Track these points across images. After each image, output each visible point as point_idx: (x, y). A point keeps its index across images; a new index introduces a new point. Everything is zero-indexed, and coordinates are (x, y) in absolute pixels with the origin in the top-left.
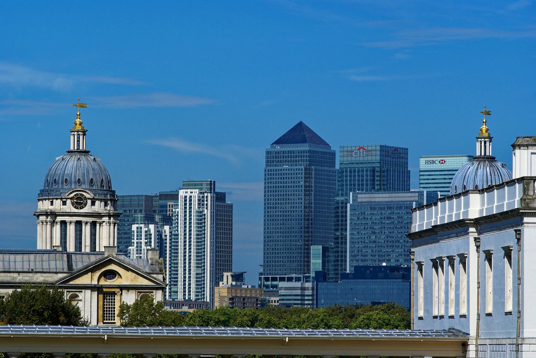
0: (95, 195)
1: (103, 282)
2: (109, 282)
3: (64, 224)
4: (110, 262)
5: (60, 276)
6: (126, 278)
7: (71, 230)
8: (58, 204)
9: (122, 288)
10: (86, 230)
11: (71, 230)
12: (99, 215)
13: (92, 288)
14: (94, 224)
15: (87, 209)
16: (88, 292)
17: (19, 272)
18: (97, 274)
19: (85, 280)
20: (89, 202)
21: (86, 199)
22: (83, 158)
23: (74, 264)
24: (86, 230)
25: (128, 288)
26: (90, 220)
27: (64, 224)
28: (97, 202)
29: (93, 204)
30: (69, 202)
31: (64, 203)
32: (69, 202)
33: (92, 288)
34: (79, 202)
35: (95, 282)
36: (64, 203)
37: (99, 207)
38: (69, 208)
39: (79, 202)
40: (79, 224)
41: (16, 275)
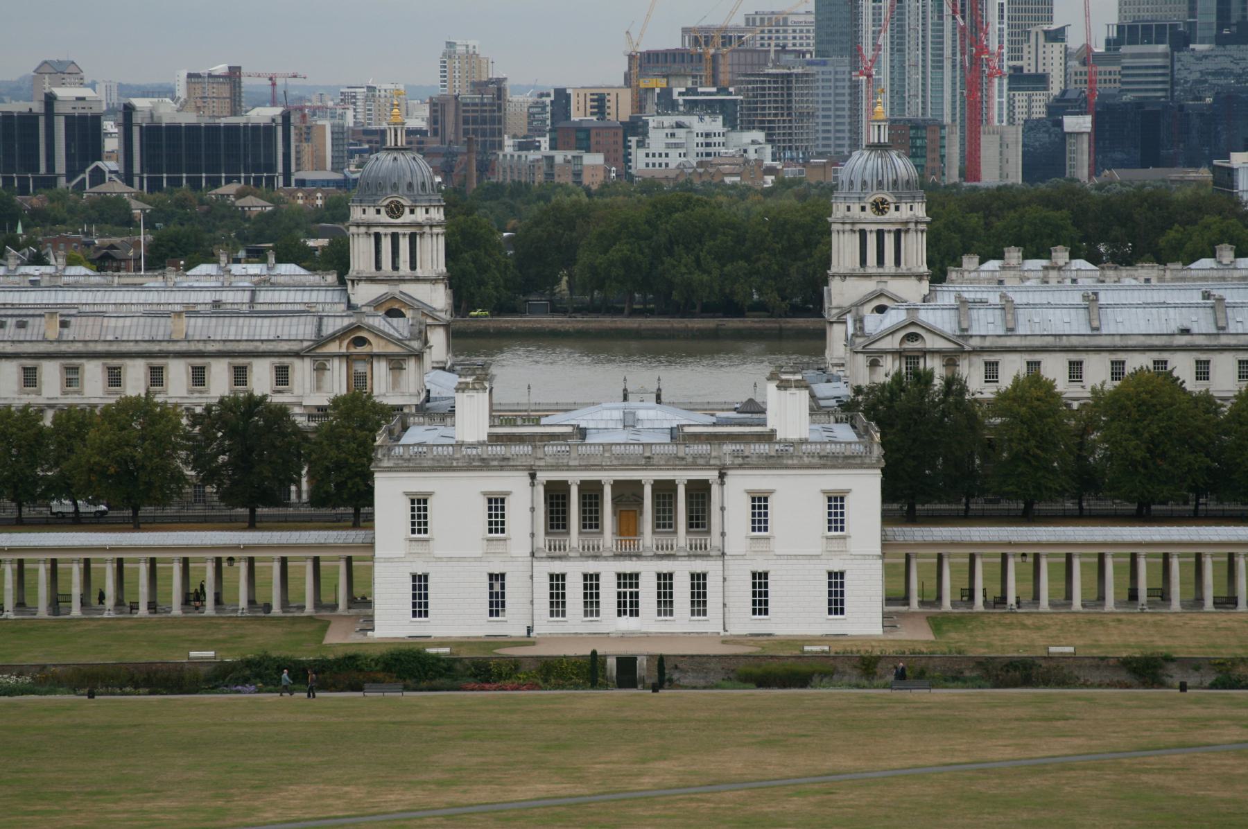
0: (415, 201)
1: (352, 350)
2: (359, 350)
3: (378, 237)
4: (359, 328)
5: (306, 344)
6: (377, 346)
7: (386, 244)
8: (371, 212)
9: (372, 357)
10: (404, 244)
11: (386, 244)
12: (420, 225)
13: (340, 356)
14: (413, 237)
15: (407, 217)
16: (336, 362)
17: (262, 341)
18: (346, 342)
19: (333, 348)
20: (407, 210)
21: (403, 206)
22: (400, 157)
23: (324, 328)
24: (404, 244)
25: (379, 356)
26: (408, 231)
27: (378, 237)
28: (418, 210)
29: (412, 212)
30: (383, 210)
31: (378, 212)
32: (383, 210)
33: (340, 356)
34: (395, 210)
35: (344, 350)
36: (378, 212)
37: (420, 216)
38: (384, 218)
39: (395, 210)
40: (395, 237)
41: (259, 344)
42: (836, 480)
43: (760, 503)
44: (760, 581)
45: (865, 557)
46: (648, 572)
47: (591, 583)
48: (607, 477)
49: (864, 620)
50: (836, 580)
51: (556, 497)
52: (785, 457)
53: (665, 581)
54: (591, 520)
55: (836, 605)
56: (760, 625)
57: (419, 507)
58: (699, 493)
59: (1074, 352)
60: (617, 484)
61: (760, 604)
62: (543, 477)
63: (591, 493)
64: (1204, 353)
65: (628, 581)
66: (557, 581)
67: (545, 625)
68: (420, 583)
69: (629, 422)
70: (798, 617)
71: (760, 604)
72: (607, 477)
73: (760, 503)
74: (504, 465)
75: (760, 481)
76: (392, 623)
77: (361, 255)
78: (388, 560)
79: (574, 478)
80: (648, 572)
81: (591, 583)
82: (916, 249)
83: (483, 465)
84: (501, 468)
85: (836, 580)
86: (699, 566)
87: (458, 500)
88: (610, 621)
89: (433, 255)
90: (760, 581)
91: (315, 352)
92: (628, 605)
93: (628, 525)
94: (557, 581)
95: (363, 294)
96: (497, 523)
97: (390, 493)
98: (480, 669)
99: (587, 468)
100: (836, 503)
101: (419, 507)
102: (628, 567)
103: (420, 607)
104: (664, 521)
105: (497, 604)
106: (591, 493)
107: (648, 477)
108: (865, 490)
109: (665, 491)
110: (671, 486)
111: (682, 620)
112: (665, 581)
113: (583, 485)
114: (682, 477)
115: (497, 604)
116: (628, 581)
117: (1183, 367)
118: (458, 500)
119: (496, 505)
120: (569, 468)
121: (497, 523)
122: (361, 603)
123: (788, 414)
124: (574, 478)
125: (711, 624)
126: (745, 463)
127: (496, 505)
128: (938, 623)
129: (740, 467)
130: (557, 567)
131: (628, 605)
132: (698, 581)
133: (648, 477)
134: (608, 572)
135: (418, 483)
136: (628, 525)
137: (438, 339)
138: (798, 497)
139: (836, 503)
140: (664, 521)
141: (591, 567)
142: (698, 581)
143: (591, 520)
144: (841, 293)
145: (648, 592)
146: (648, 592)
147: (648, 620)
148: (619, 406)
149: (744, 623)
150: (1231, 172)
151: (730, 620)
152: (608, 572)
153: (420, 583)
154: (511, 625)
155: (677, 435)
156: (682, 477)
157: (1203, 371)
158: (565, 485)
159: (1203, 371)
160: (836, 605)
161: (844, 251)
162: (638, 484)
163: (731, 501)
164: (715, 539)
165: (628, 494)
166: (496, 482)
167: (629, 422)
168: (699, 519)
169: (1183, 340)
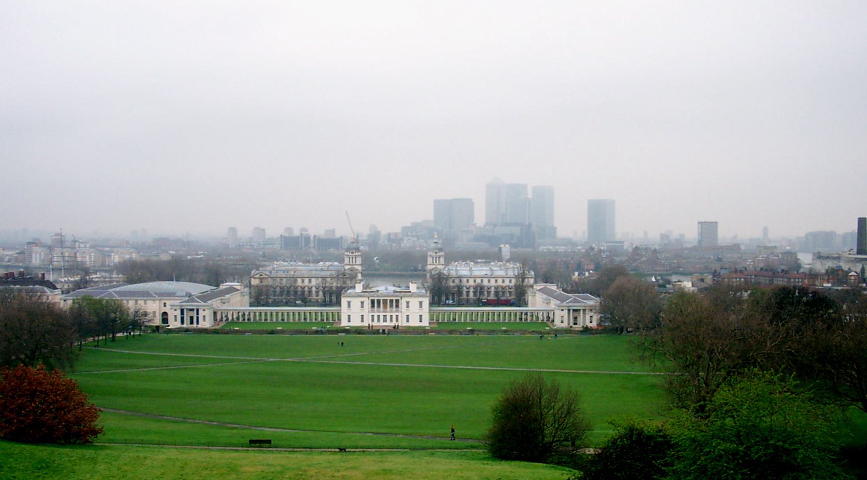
42: (421, 299)
43: (408, 303)
46: (388, 315)
47: (379, 316)
49: (425, 323)
51: (373, 302)
52: (411, 296)
53: (391, 316)
54: (379, 306)
55: (421, 321)
56: (408, 324)
57: (349, 303)
58: (397, 301)
59: (468, 278)
61: (408, 321)
64: (489, 279)
65: (385, 316)
66: (373, 316)
68: (349, 316)
69: (386, 289)
70: (414, 323)
71: (408, 321)
73: (408, 303)
74: (364, 296)
76: (344, 323)
77: (347, 261)
79: (376, 299)
80: (388, 315)
81: (379, 316)
82: (442, 260)
83: (361, 296)
85: (421, 316)
88: (382, 323)
89: (359, 261)
91: (337, 277)
92: (385, 321)
93: (385, 307)
94: (373, 316)
95: (347, 267)
96: (362, 307)
97: (344, 301)
98: (358, 331)
100: (421, 303)
101: (349, 303)
103: (349, 321)
104: (391, 306)
105: (362, 321)
106: (379, 301)
107: (388, 298)
108: (426, 301)
109: (391, 301)
112: (391, 316)
114: (394, 299)
115: (362, 321)
116: (385, 316)
117: (485, 282)
118: (356, 302)
119: (362, 303)
121: (362, 307)
122: (339, 319)
123: (413, 287)
124: (376, 299)
126: (405, 296)
127: (362, 303)
128: (439, 323)
131: (385, 321)
132: (397, 316)
133: (388, 298)
134: (382, 315)
135: (349, 299)
136: (385, 307)
137: (360, 276)
138: (414, 302)
139: (421, 303)
140: (391, 306)
142: (397, 316)
143: (379, 306)
144: (429, 267)
145: (388, 318)
146: (388, 318)
147: (388, 323)
148: (385, 288)
149: (405, 324)
150: (500, 249)
151: (402, 323)
152: (382, 315)
153: (349, 316)
155: (395, 292)
157: (489, 281)
159: (489, 281)
160: (421, 321)
161: (430, 260)
165: (385, 301)
166: (362, 299)
167: (386, 289)
168: (397, 306)
169: (486, 276)
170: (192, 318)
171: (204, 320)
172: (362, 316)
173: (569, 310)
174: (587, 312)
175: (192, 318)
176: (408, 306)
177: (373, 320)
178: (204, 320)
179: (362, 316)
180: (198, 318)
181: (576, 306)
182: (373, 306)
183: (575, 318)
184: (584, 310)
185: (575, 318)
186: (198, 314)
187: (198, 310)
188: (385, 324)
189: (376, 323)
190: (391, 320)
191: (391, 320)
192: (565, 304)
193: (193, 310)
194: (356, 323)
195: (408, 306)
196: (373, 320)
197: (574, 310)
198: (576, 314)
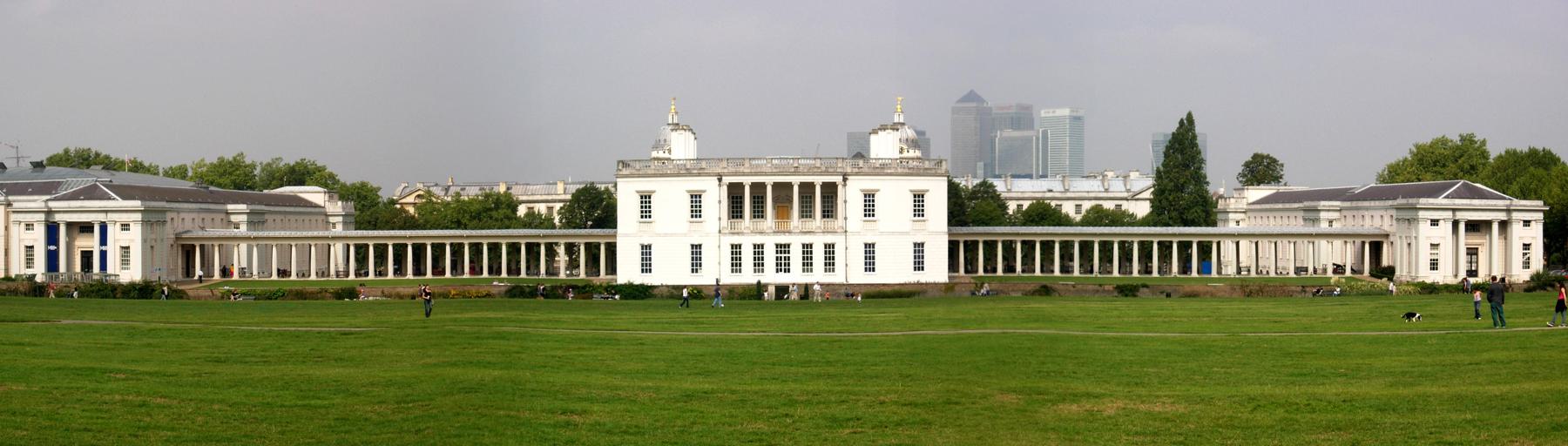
42: (919, 183)
43: (869, 199)
44: (870, 248)
45: (937, 233)
47: (759, 249)
48: (769, 180)
50: (919, 248)
52: (882, 170)
53: (807, 249)
54: (758, 212)
55: (919, 265)
57: (646, 199)
58: (830, 191)
60: (776, 186)
61: (870, 266)
62: (727, 180)
63: (758, 189)
65: (783, 248)
66: (736, 249)
67: (729, 279)
68: (646, 250)
70: (894, 270)
71: (870, 266)
72: (769, 180)
73: (869, 199)
75: (869, 183)
78: (626, 235)
79: (747, 181)
83: (688, 173)
84: (699, 175)
85: (919, 248)
86: (829, 239)
87: (671, 195)
90: (870, 248)
92: (783, 265)
94: (736, 249)
99: (756, 174)
100: (919, 198)
101: (646, 199)
102: (783, 239)
104: (806, 212)
105: (696, 264)
107: (796, 180)
109: (807, 189)
110: (811, 185)
111: (818, 276)
112: (807, 249)
113: (754, 186)
114: (818, 180)
115: (696, 264)
116: (783, 248)
118: (671, 195)
119: (696, 198)
120: (744, 174)
124: (747, 181)
125: (837, 277)
127: (696, 198)
129: (857, 174)
130: (736, 240)
131: (783, 265)
132: (829, 249)
133: (796, 180)
135: (645, 185)
138: (894, 194)
139: (919, 198)
140: (806, 212)
141: (759, 240)
142: (829, 249)
143: (758, 212)
149: (859, 277)
151: (850, 271)
153: (646, 250)
154: (706, 278)
156: (818, 180)
158: (741, 186)
160: (919, 265)
162: (789, 186)
163: (851, 196)
164: (839, 222)
165: (782, 190)
166: (696, 184)
168: (829, 212)
170: (87, 256)
171: (125, 261)
172: (696, 249)
173: (1456, 224)
174: (1517, 229)
175: (87, 256)
176: (869, 209)
177: (736, 264)
178: (125, 261)
179: (696, 249)
180: (103, 255)
181: (1476, 209)
182: (736, 211)
183: (1472, 252)
184: (1504, 225)
185: (1472, 252)
186: (103, 241)
187: (104, 228)
188: (783, 278)
189: (747, 277)
190: (807, 264)
191: (807, 264)
192: (1441, 201)
193: (86, 228)
194: (671, 271)
195: (869, 209)
196: (736, 264)
197: (1473, 227)
198: (1475, 240)
